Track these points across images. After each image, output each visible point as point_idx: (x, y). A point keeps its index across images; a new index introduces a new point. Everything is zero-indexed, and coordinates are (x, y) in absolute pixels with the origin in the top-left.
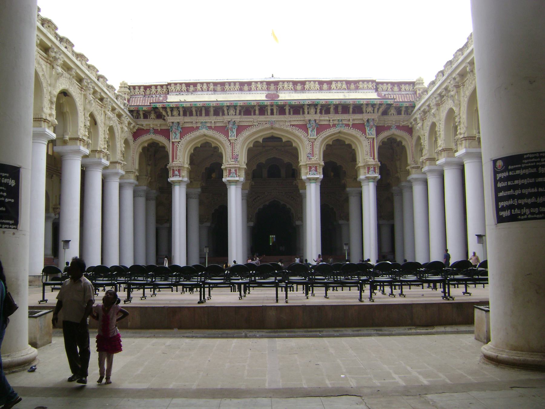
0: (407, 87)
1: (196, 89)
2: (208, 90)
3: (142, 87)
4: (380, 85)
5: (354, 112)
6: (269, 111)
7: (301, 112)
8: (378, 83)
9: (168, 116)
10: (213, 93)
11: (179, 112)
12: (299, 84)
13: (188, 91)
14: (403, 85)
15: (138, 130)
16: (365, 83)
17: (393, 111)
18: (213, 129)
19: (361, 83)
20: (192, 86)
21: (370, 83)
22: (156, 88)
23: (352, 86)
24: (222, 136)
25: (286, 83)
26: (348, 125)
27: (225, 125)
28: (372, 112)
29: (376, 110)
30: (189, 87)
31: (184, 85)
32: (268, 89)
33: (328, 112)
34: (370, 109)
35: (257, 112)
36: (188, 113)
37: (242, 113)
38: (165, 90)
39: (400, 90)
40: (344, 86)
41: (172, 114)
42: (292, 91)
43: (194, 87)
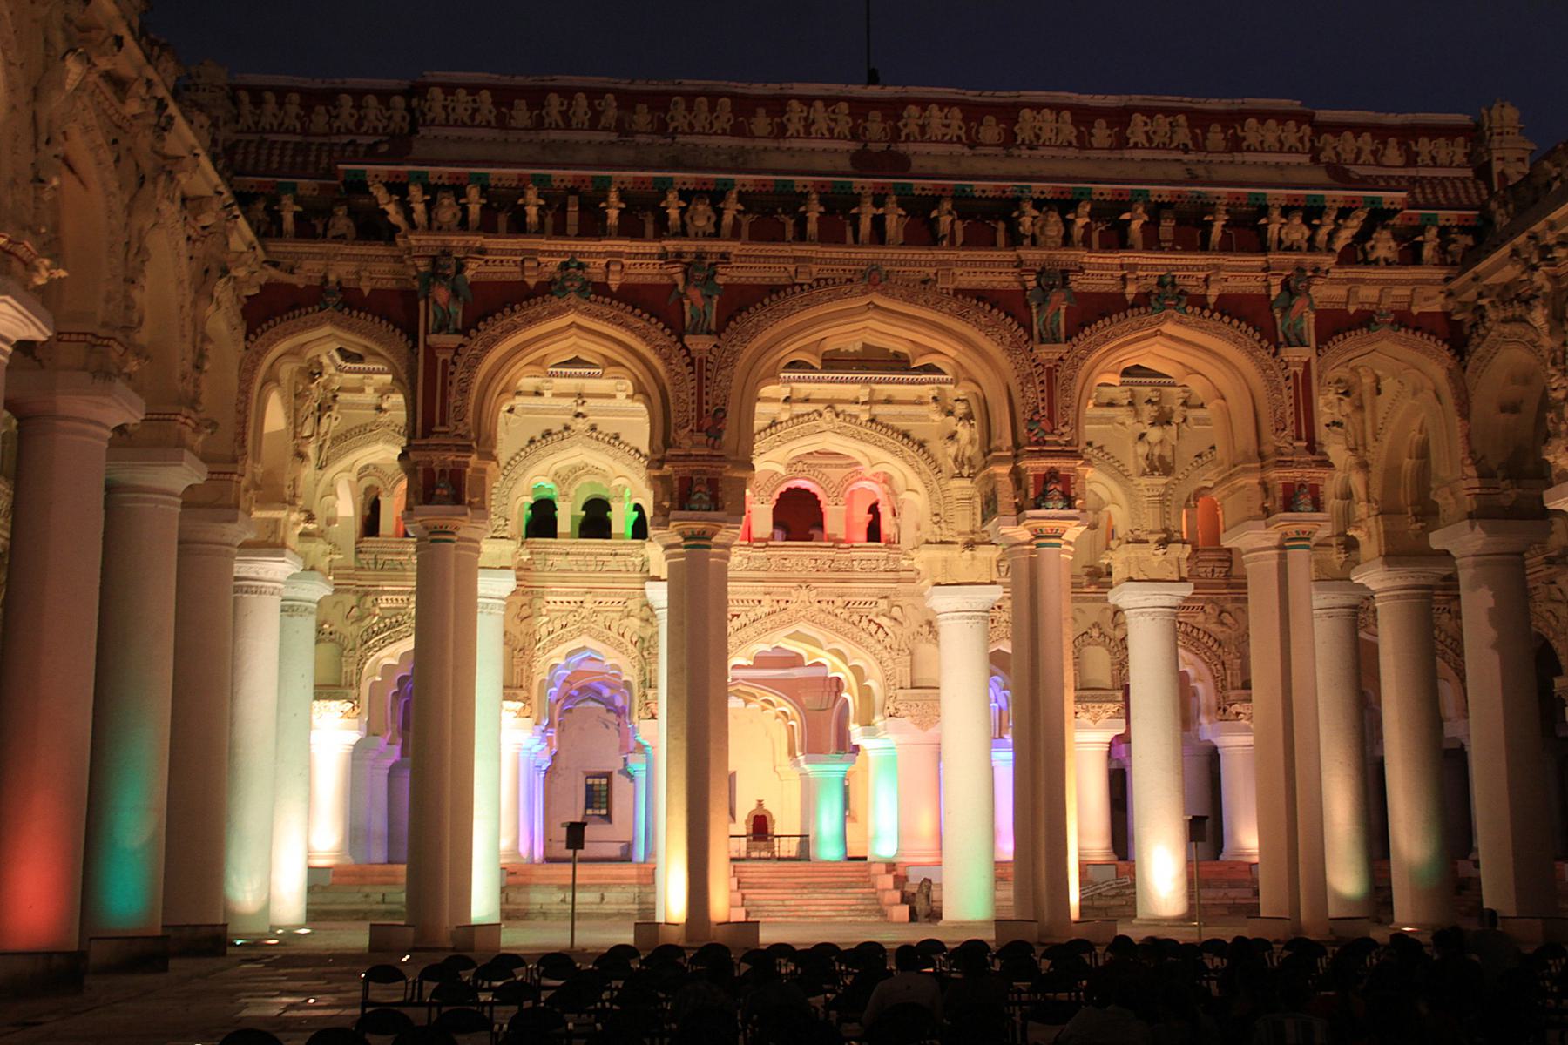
0: (1442, 149)
1: (541, 118)
2: (594, 125)
3: (295, 97)
4: (1327, 138)
5: (1226, 247)
6: (865, 225)
7: (1001, 237)
8: (1319, 128)
9: (413, 226)
10: (613, 137)
11: (464, 209)
12: (990, 119)
13: (502, 123)
14: (1424, 141)
15: (266, 288)
16: (1272, 123)
17: (1384, 245)
18: (613, 296)
19: (1252, 122)
20: (521, 104)
21: (1292, 124)
22: (358, 106)
23: (1216, 136)
24: (656, 329)
25: (934, 109)
26: (1200, 302)
27: (665, 280)
28: (1305, 246)
29: (1322, 235)
30: (511, 106)
31: (485, 95)
32: (854, 136)
33: (1117, 239)
34: (1297, 232)
35: (812, 227)
36: (502, 220)
37: (745, 231)
38: (397, 117)
39: (1411, 160)
40: (1183, 135)
41: (430, 220)
42: (957, 148)
43: (530, 108)
